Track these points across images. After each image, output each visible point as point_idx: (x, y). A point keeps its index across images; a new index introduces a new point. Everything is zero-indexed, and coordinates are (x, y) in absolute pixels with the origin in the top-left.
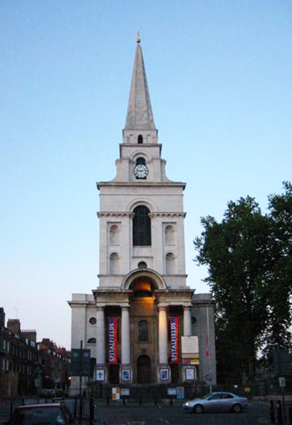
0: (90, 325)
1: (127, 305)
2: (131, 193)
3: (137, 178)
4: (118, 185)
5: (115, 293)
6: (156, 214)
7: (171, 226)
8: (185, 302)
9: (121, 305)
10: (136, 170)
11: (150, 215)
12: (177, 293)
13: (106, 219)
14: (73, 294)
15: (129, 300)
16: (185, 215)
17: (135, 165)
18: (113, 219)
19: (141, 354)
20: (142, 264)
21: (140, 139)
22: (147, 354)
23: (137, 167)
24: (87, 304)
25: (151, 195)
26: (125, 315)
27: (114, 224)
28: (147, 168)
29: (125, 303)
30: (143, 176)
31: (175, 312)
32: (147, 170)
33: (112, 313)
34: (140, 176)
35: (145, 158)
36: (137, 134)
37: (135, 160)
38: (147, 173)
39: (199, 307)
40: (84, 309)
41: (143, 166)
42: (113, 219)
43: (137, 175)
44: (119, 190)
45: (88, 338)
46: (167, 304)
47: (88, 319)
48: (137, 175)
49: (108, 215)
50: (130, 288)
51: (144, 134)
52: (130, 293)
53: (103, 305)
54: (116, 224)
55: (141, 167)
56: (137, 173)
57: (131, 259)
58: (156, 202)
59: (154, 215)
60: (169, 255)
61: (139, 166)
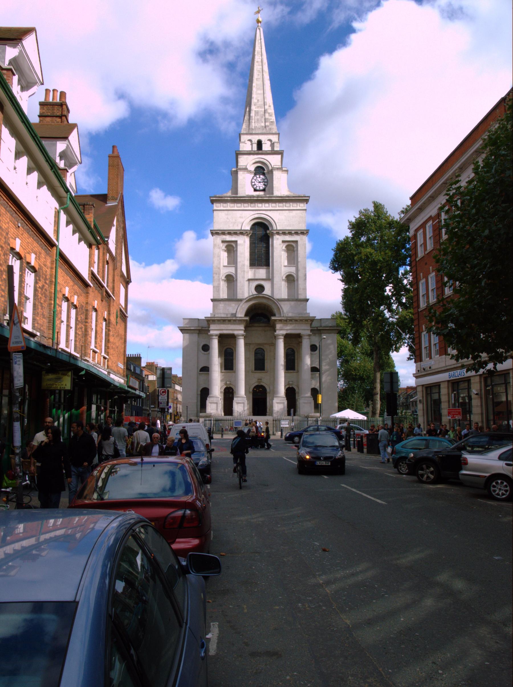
0: (203, 352)
1: (242, 332)
2: (250, 208)
3: (255, 190)
5: (230, 321)
7: (292, 246)
8: (304, 330)
9: (236, 333)
10: (253, 181)
12: (296, 320)
13: (219, 239)
17: (253, 175)
18: (228, 238)
19: (256, 384)
20: (260, 288)
21: (260, 144)
22: (262, 384)
23: (255, 178)
24: (199, 330)
26: (241, 343)
28: (266, 178)
29: (239, 330)
30: (261, 188)
31: (293, 341)
32: (266, 180)
33: (227, 343)
34: (258, 188)
36: (255, 139)
38: (266, 184)
39: (321, 334)
40: (197, 335)
41: (261, 176)
42: (228, 238)
43: (255, 187)
44: (236, 204)
45: (200, 367)
46: (284, 332)
47: (201, 347)
48: (255, 187)
50: (246, 315)
51: (264, 138)
52: (244, 320)
53: (218, 332)
55: (260, 177)
56: (255, 185)
57: (248, 282)
60: (290, 279)
61: (258, 176)
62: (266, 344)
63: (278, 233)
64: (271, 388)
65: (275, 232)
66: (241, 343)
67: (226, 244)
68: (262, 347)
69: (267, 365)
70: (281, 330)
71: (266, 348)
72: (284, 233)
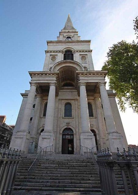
4: (59, 42)
6: (76, 51)
7: (84, 57)
11: (73, 52)
13: (49, 54)
14: (25, 90)
15: (56, 79)
16: (92, 51)
22: (70, 127)
25: (73, 45)
26: (52, 89)
27: (54, 56)
29: (52, 80)
35: (71, 36)
37: (66, 37)
42: (53, 54)
46: (86, 81)
49: (51, 52)
54: (55, 56)
58: (74, 47)
59: (75, 51)
62: (72, 99)
63: (77, 52)
64: (77, 130)
65: (76, 51)
66: (52, 89)
67: (52, 56)
68: (69, 101)
69: (74, 113)
70: (83, 80)
71: (72, 102)
72: (80, 51)
